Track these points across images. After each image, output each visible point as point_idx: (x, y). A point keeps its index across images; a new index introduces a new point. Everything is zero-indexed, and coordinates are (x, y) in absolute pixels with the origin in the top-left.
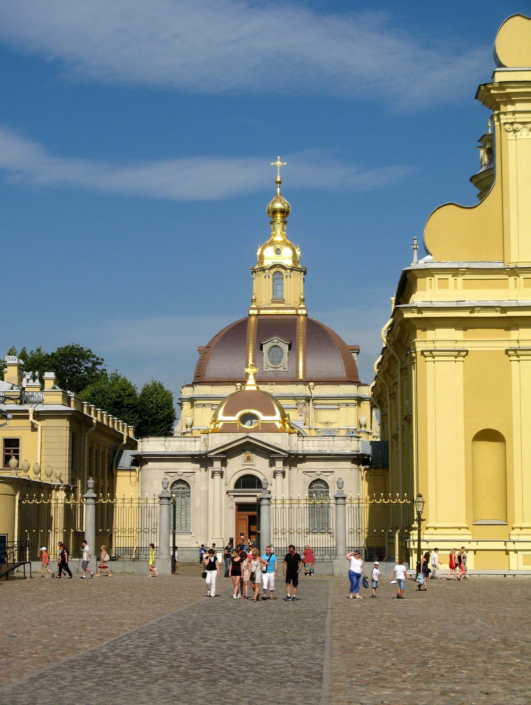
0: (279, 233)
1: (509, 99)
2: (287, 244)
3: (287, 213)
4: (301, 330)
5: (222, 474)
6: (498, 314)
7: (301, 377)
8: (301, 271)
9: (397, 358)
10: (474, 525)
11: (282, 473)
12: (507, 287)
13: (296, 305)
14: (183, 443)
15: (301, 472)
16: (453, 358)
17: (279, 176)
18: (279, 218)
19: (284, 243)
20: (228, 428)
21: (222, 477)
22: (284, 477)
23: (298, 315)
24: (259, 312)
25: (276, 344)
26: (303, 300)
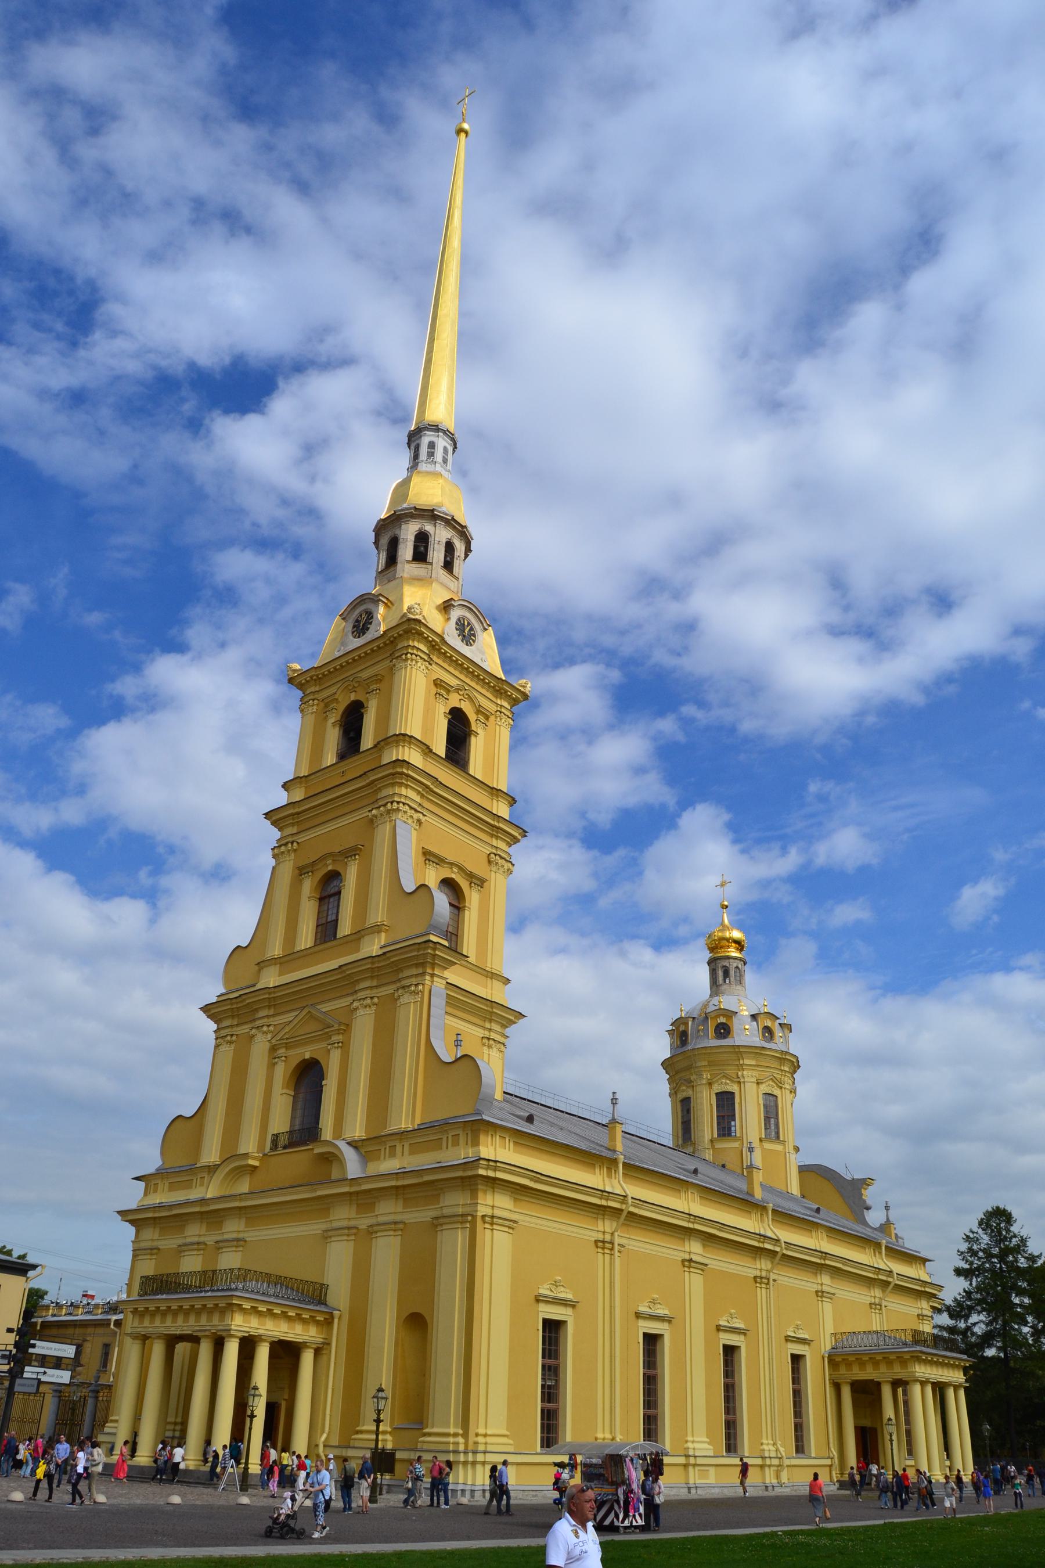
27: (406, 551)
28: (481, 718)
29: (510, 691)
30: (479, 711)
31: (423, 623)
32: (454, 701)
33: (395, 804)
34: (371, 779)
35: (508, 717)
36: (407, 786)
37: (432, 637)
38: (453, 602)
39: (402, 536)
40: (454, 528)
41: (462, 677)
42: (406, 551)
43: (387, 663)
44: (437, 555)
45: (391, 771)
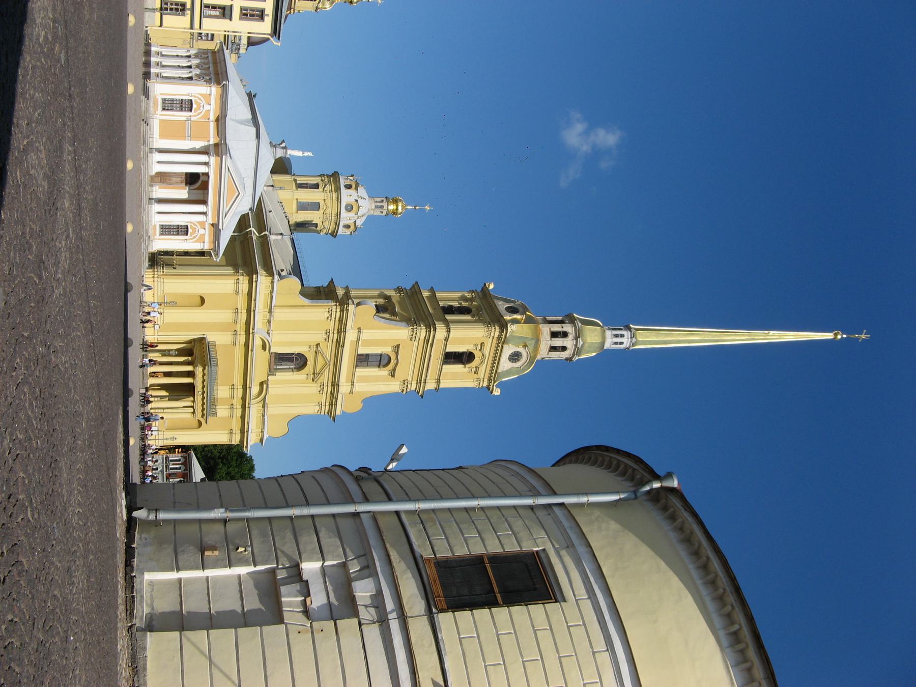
1: (342, 311)
9: (242, 234)
12: (264, 308)
27: (557, 328)
28: (474, 369)
29: (492, 384)
32: (477, 354)
33: (416, 327)
34: (429, 318)
35: (479, 385)
36: (426, 332)
37: (503, 337)
38: (527, 348)
39: (563, 325)
40: (575, 350)
41: (491, 359)
42: (557, 328)
43: (488, 320)
44: (558, 342)
45: (431, 323)
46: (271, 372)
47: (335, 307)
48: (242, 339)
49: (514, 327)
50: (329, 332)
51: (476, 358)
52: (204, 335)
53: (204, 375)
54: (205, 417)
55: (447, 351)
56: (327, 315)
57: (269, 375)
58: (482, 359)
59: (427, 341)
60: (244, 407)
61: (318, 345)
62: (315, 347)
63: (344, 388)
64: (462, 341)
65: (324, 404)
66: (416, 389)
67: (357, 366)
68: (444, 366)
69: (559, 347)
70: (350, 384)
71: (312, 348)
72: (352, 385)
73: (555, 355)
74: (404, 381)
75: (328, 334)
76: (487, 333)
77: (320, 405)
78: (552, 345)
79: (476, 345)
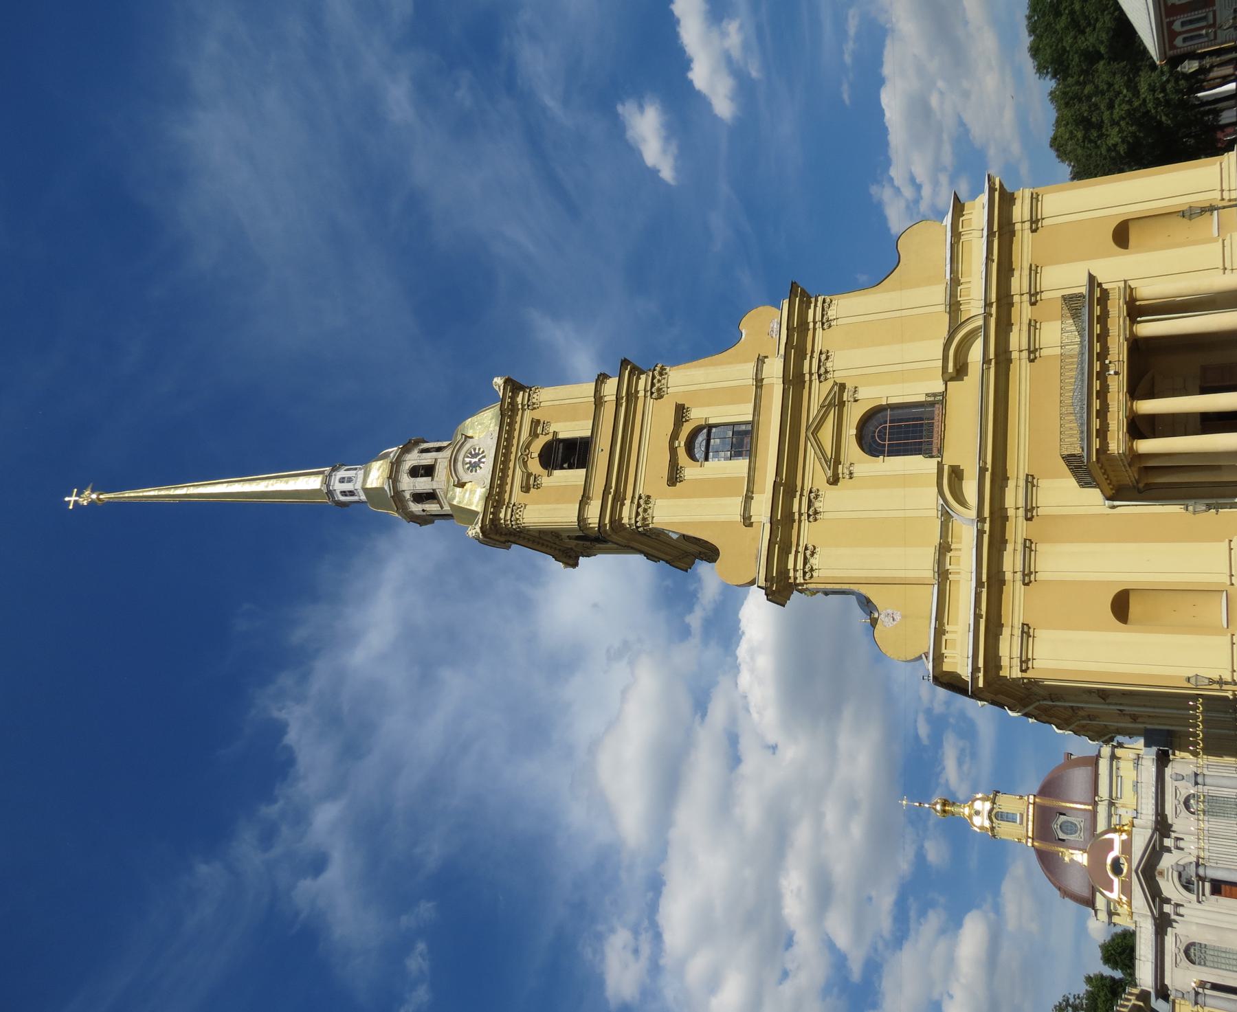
0: (962, 810)
1: (783, 572)
2: (972, 804)
3: (945, 800)
4: (1048, 802)
5: (1177, 905)
6: (985, 590)
7: (1090, 807)
8: (996, 795)
10: (1228, 627)
11: (1177, 841)
12: (958, 581)
13: (1026, 803)
14: (1143, 941)
15: (1175, 821)
16: (1031, 639)
17: (915, 804)
18: (950, 808)
19: (971, 806)
20: (1126, 889)
21: (1182, 905)
22: (1182, 839)
23: (1034, 803)
24: (1030, 838)
25: (1059, 827)
26: (1021, 797)
30: (534, 435)
31: (482, 524)
35: (529, 395)
36: (621, 518)
40: (397, 472)
46: (938, 402)
47: (798, 581)
48: (1013, 497)
49: (470, 533)
50: (809, 516)
51: (535, 455)
52: (1113, 507)
53: (1103, 433)
54: (1097, 293)
55: (585, 470)
56: (814, 561)
57: (944, 394)
58: (527, 455)
59: (619, 499)
60: (1004, 301)
61: (834, 481)
62: (841, 476)
63: (774, 369)
64: (560, 495)
65: (819, 325)
66: (638, 378)
67: (751, 423)
68: (588, 433)
69: (422, 476)
70: (764, 382)
71: (846, 472)
72: (759, 382)
73: (427, 459)
74: (661, 397)
75: (811, 513)
76: (517, 516)
77: (826, 323)
78: (430, 478)
79: (538, 487)
